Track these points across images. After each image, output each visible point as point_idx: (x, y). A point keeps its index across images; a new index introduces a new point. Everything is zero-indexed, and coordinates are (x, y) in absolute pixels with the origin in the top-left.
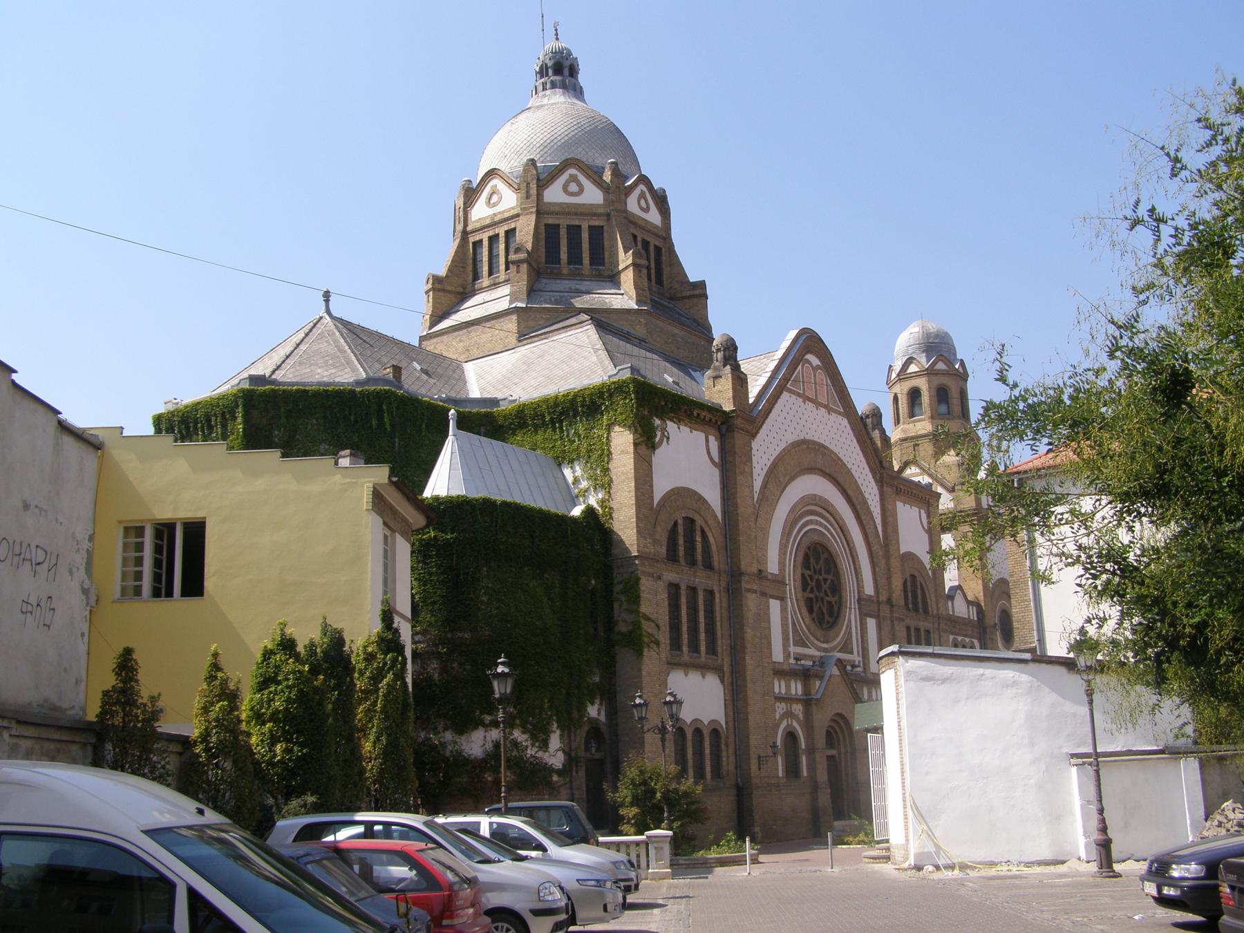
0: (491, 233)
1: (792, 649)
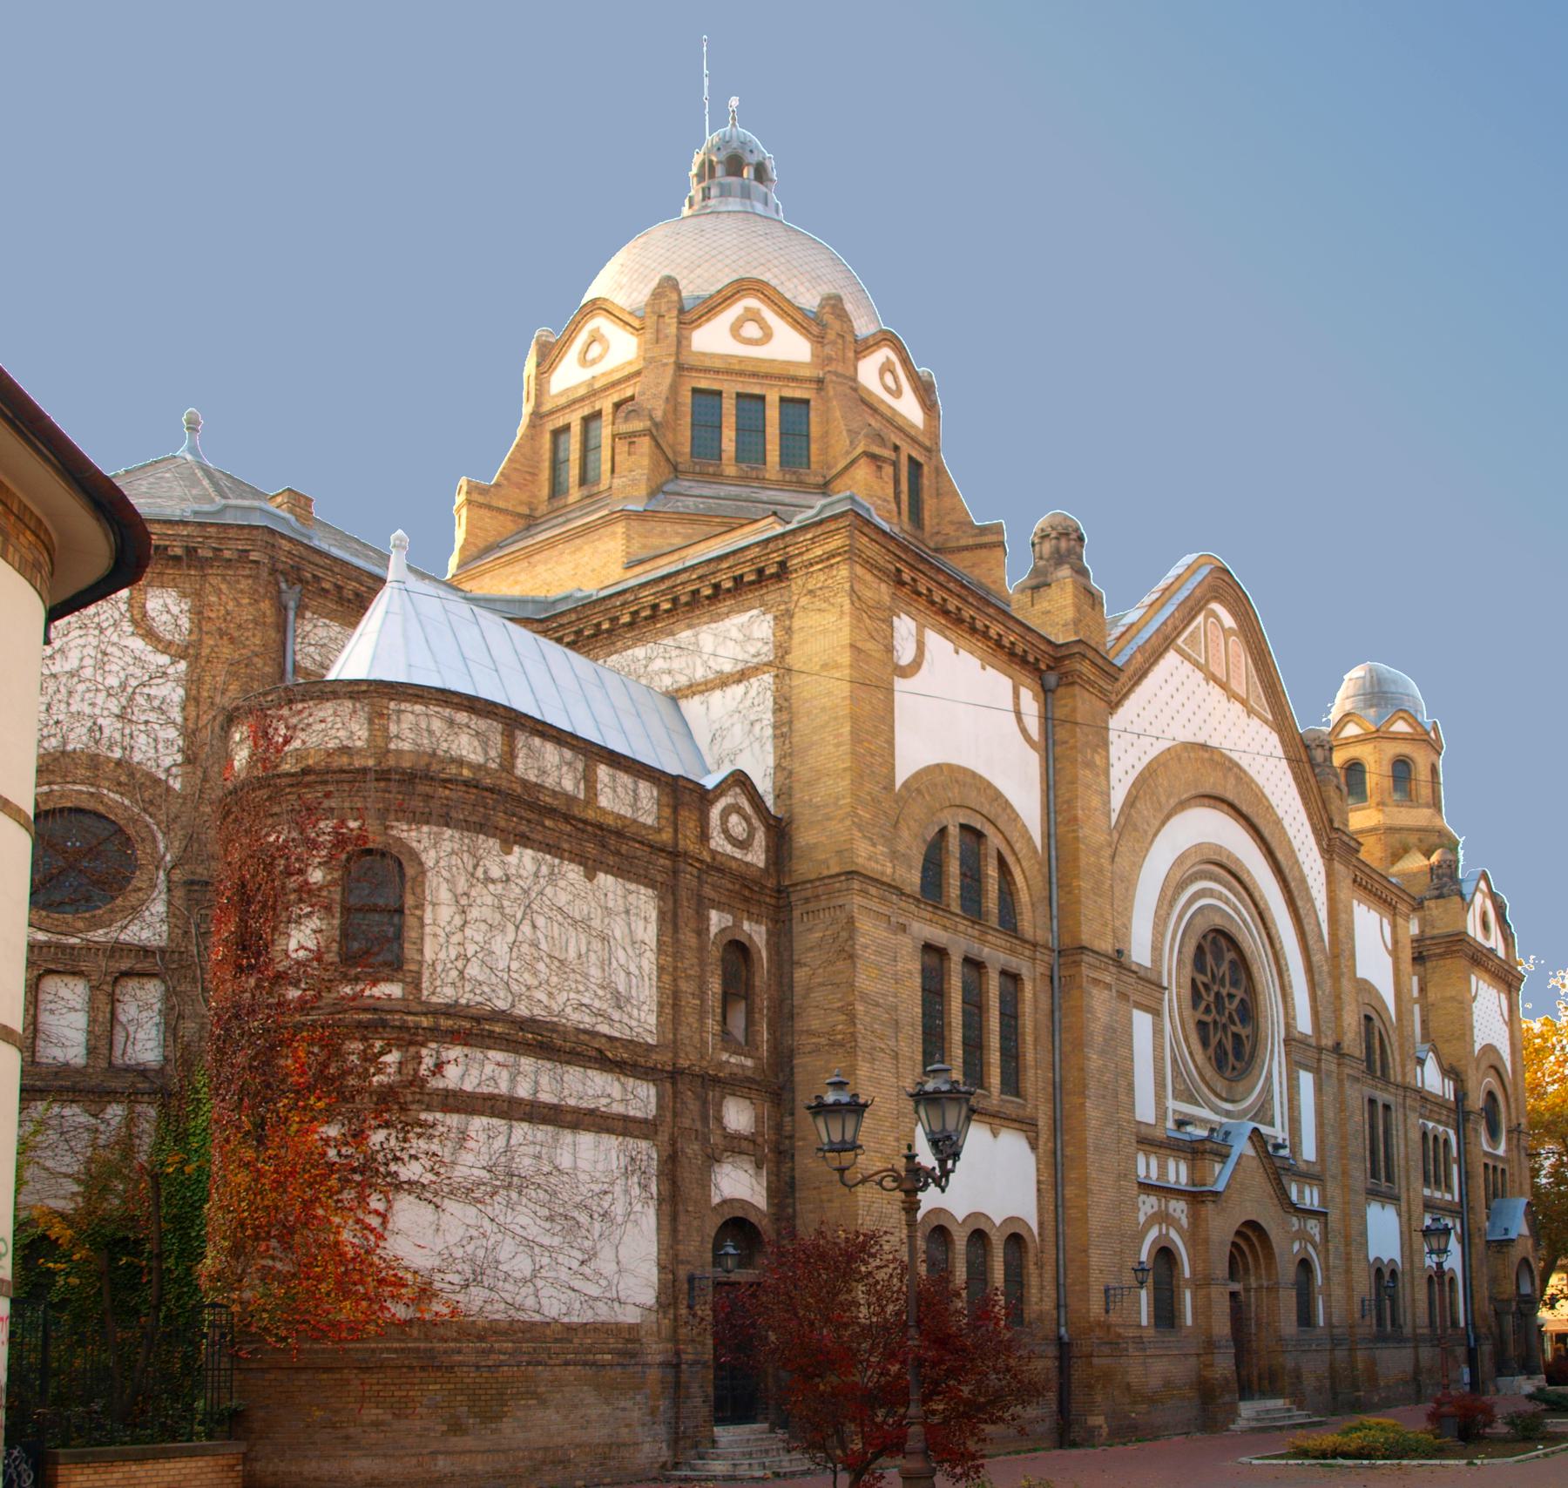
1: (1171, 1104)
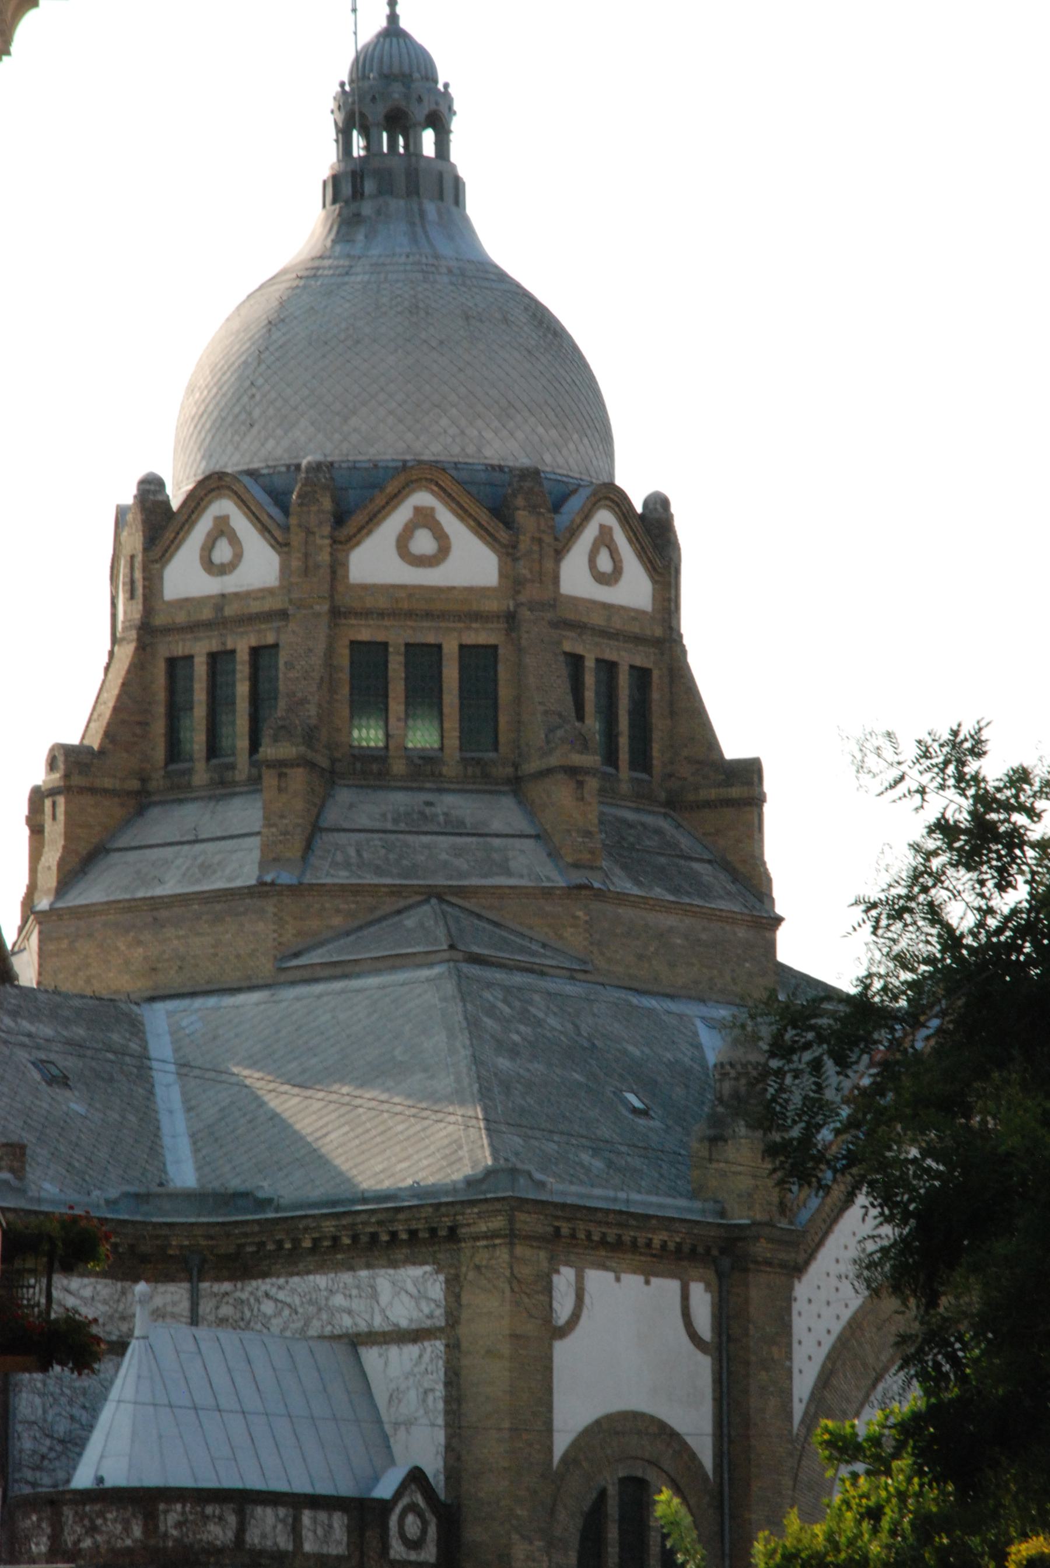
0: (214, 646)
